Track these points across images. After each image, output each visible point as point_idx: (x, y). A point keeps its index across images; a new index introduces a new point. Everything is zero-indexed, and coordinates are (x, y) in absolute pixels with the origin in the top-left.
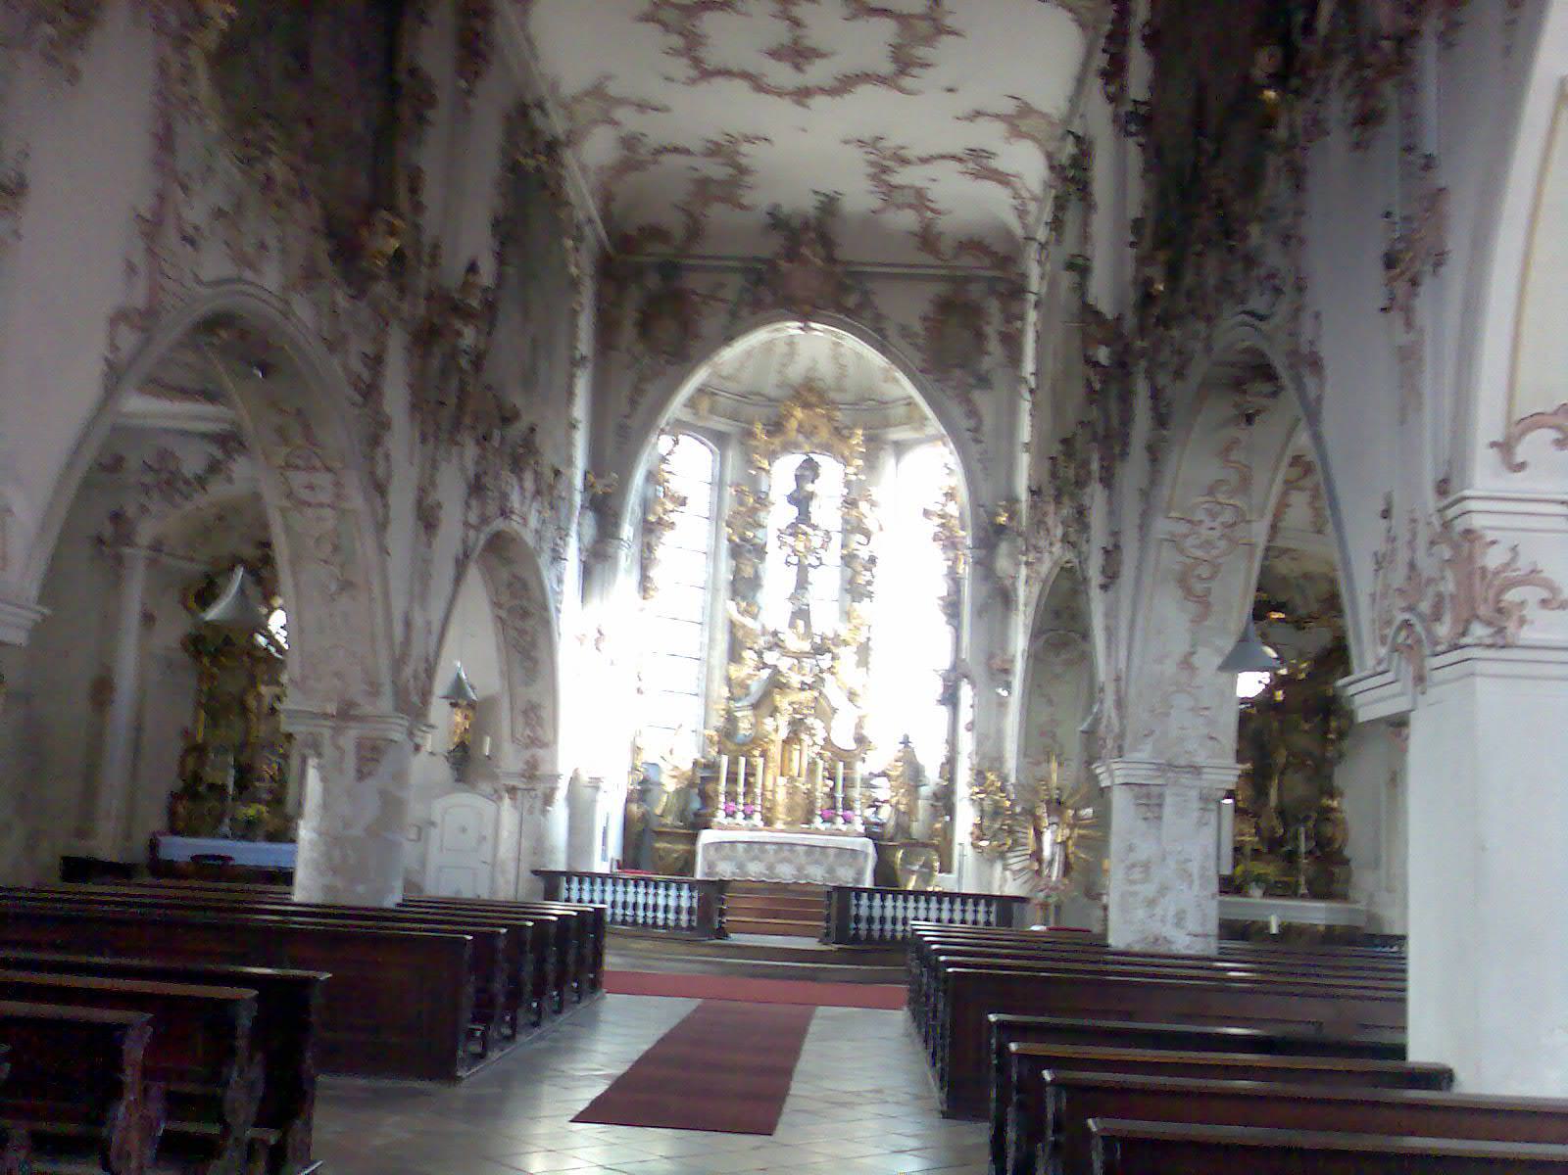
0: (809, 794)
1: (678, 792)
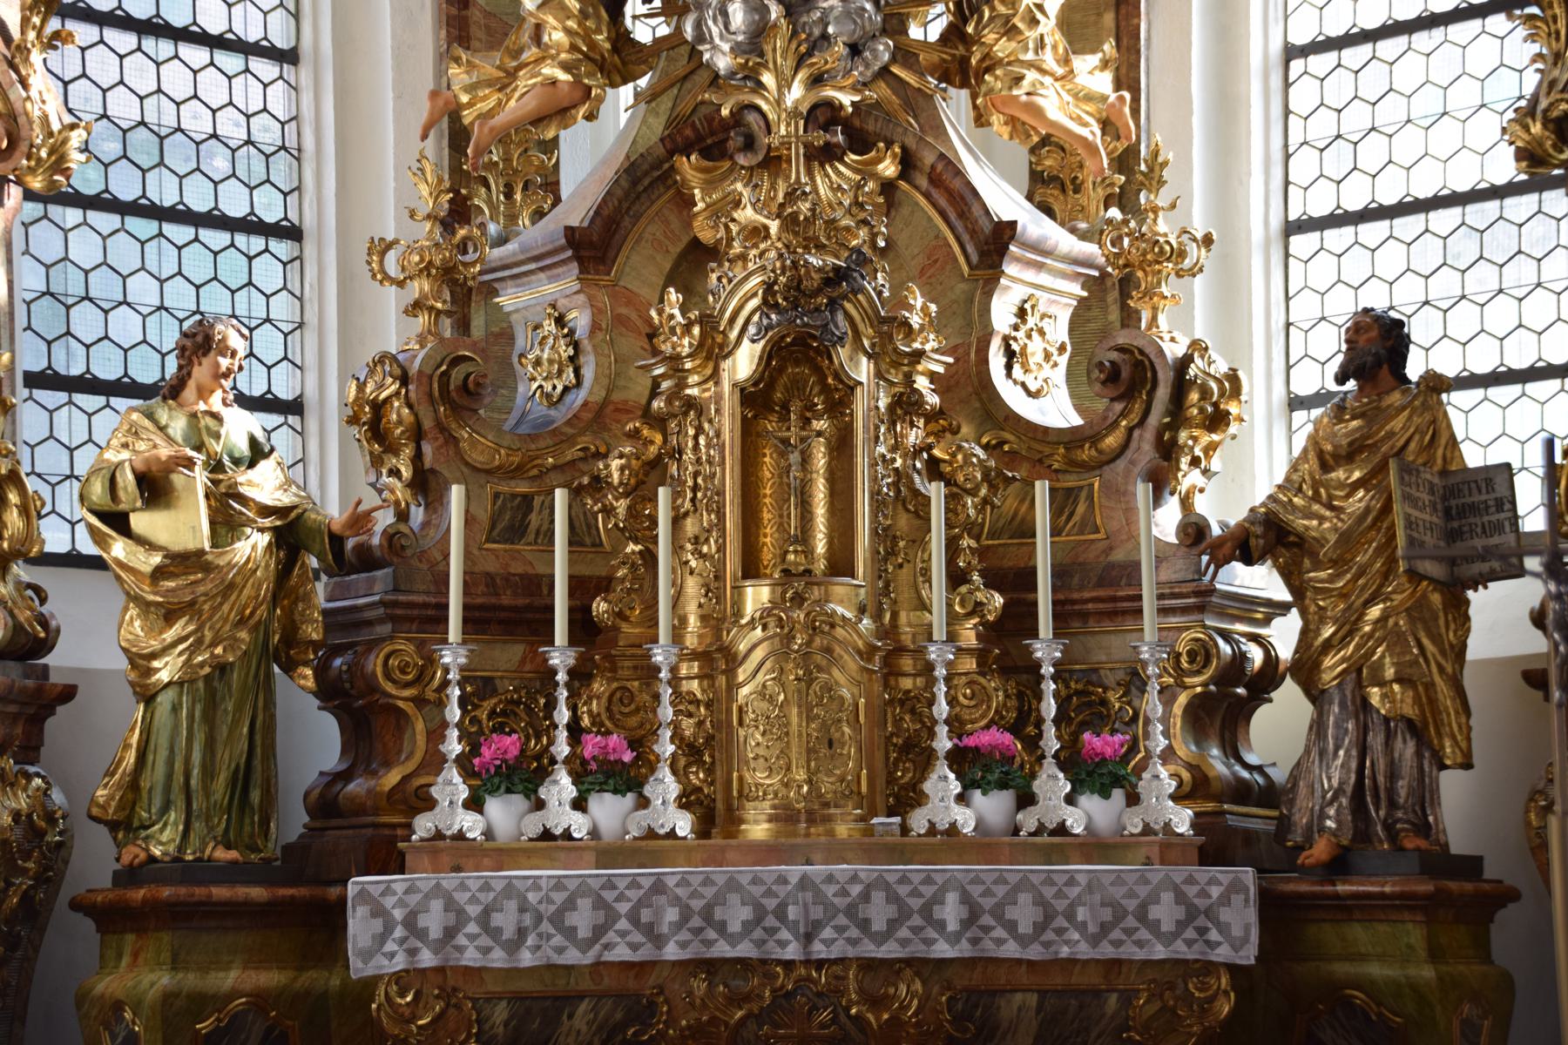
0: (892, 654)
1: (207, 687)
